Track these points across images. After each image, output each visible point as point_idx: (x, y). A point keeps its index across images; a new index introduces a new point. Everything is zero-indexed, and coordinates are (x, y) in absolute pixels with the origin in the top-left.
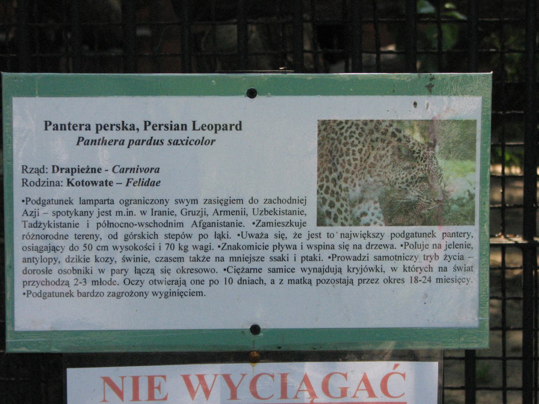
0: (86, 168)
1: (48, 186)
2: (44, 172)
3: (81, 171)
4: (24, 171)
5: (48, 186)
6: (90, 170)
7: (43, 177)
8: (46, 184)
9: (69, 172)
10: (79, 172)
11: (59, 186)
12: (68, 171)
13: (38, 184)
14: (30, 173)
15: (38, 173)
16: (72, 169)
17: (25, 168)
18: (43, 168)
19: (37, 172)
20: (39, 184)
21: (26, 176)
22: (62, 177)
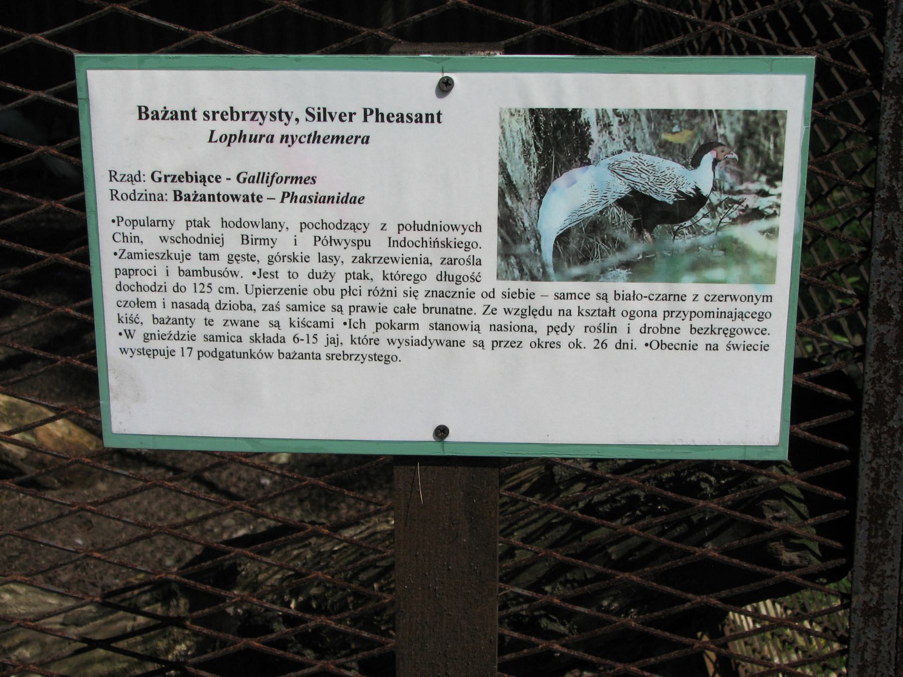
1: (146, 200)
2: (140, 181)
4: (113, 178)
5: (146, 200)
7: (139, 187)
8: (144, 197)
11: (162, 200)
13: (133, 197)
14: (121, 181)
15: (132, 181)
17: (113, 174)
18: (139, 175)
19: (130, 179)
20: (133, 197)
21: (115, 185)
22: (168, 188)
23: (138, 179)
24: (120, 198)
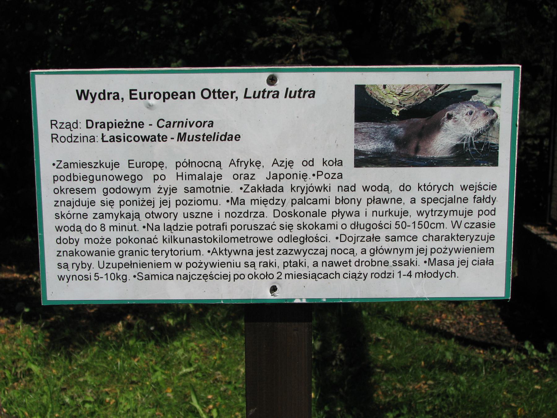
0: (125, 122)
3: (120, 125)
6: (130, 125)
7: (76, 132)
9: (104, 127)
10: (116, 127)
12: (103, 125)
16: (108, 123)
20: (72, 139)
21: (55, 130)
22: (97, 132)
23: (75, 126)
24: (59, 141)
